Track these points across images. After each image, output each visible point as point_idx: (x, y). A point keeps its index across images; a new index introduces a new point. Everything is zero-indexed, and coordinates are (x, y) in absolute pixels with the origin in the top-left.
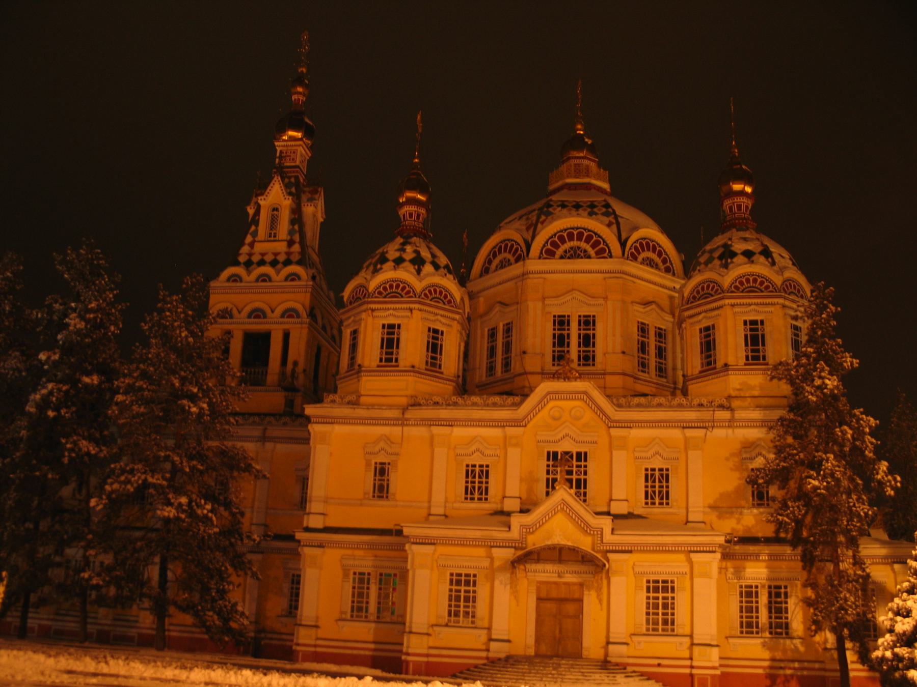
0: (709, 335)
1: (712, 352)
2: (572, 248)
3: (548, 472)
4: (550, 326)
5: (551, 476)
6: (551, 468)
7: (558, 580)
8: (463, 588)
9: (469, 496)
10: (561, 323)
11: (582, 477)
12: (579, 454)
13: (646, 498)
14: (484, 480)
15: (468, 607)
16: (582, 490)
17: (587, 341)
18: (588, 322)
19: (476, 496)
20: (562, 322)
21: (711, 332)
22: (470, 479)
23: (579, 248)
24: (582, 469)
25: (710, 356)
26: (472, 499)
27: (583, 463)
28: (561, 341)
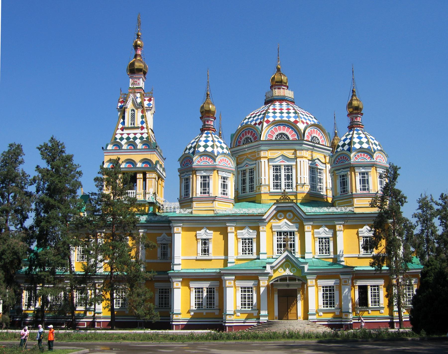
0: (344, 179)
1: (346, 187)
2: (280, 134)
3: (278, 241)
4: (271, 171)
5: (279, 243)
6: (279, 239)
7: (286, 288)
8: (247, 294)
9: (244, 253)
10: (277, 169)
11: (292, 243)
12: (291, 233)
13: (320, 251)
14: (250, 245)
15: (244, 301)
16: (293, 248)
17: (288, 177)
18: (289, 168)
19: (247, 252)
20: (277, 168)
21: (345, 177)
22: (244, 245)
23: (284, 134)
24: (292, 239)
25: (344, 188)
26: (246, 254)
27: (292, 237)
28: (277, 177)
